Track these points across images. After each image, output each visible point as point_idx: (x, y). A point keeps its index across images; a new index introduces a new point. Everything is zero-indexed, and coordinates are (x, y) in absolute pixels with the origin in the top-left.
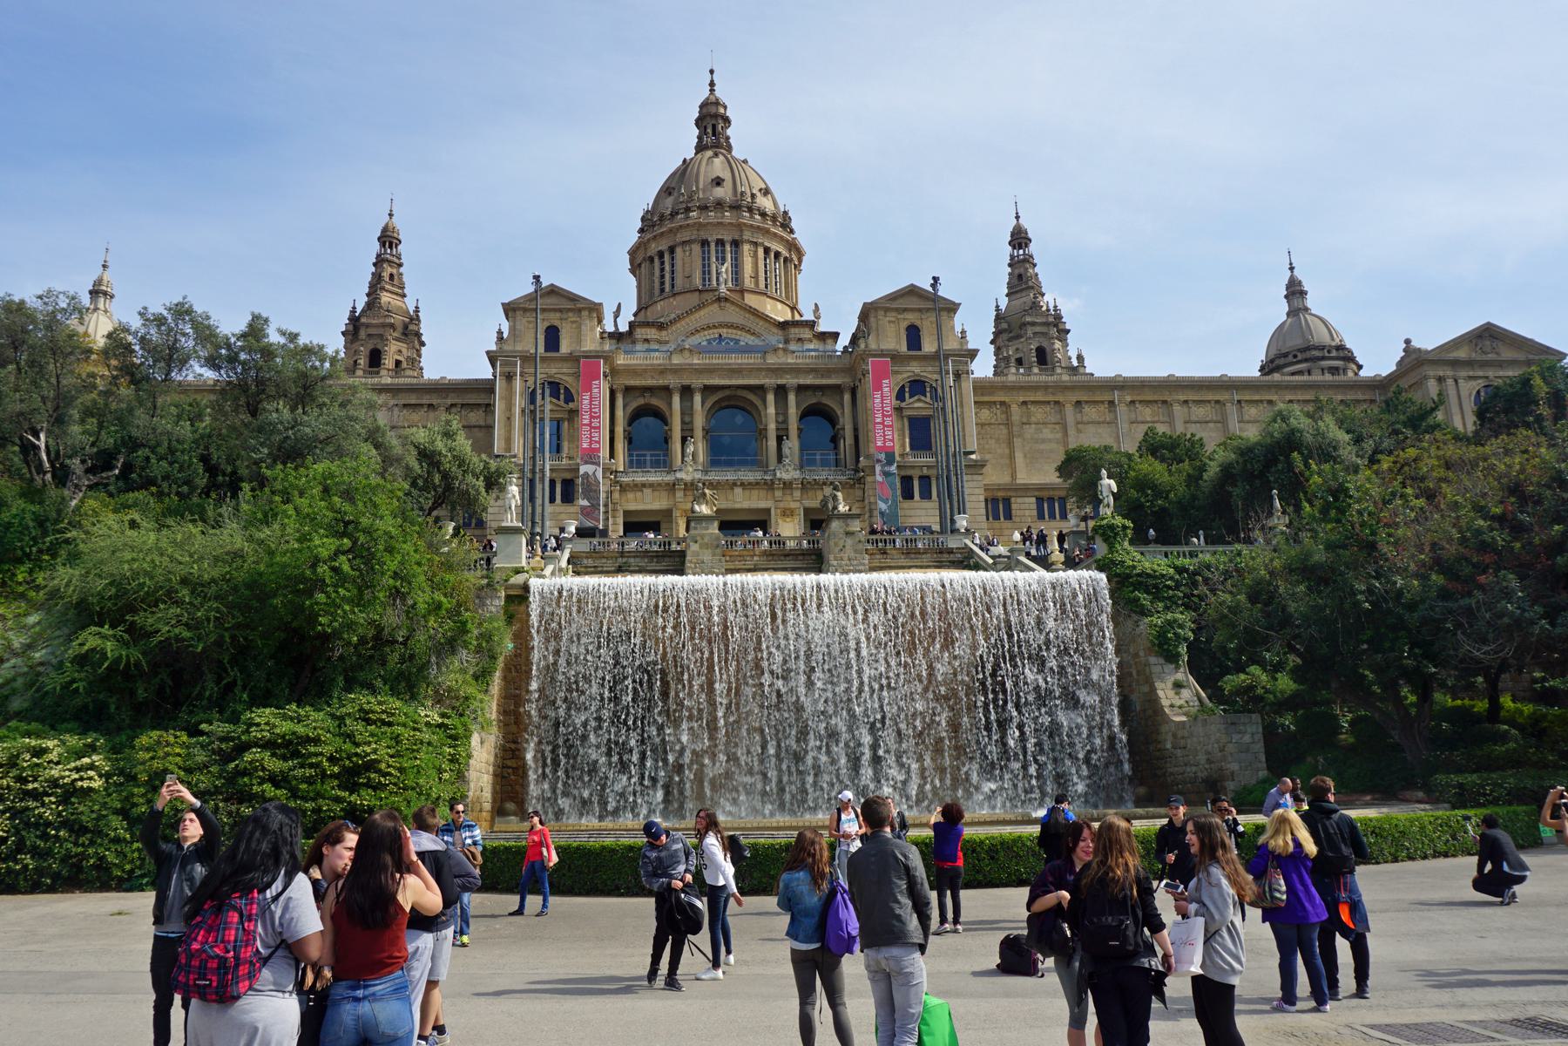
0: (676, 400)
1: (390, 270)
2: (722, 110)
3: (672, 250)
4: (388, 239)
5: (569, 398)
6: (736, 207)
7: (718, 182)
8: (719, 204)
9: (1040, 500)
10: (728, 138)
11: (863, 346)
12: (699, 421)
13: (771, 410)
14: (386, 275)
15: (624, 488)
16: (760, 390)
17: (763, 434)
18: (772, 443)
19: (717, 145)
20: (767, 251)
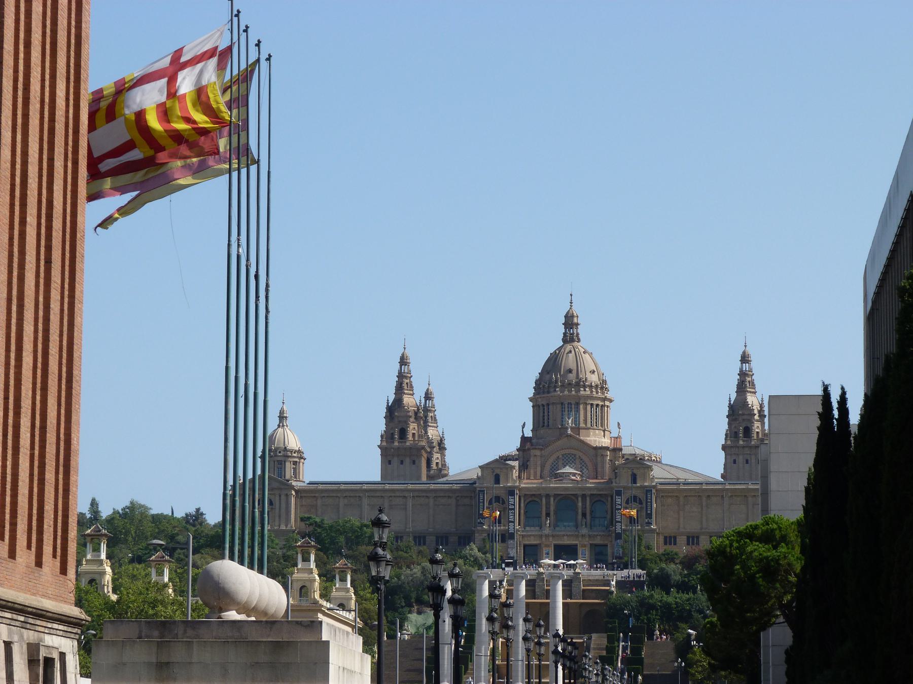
0: (544, 500)
1: (406, 381)
2: (575, 320)
3: (548, 405)
4: (403, 361)
5: (504, 502)
6: (578, 385)
7: (570, 371)
8: (570, 384)
9: (688, 538)
10: (578, 334)
11: (614, 484)
12: (552, 508)
13: (580, 504)
14: (405, 385)
15: (523, 536)
16: (576, 496)
17: (577, 513)
18: (580, 517)
19: (572, 340)
20: (592, 405)
